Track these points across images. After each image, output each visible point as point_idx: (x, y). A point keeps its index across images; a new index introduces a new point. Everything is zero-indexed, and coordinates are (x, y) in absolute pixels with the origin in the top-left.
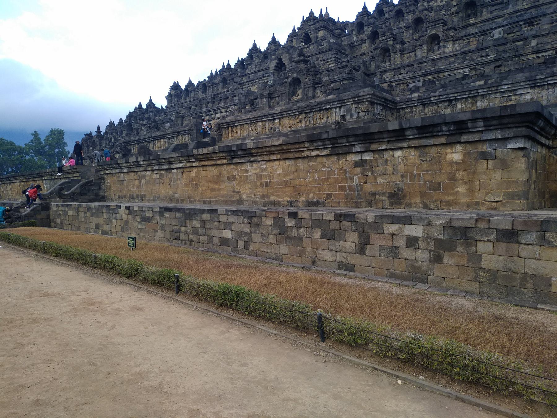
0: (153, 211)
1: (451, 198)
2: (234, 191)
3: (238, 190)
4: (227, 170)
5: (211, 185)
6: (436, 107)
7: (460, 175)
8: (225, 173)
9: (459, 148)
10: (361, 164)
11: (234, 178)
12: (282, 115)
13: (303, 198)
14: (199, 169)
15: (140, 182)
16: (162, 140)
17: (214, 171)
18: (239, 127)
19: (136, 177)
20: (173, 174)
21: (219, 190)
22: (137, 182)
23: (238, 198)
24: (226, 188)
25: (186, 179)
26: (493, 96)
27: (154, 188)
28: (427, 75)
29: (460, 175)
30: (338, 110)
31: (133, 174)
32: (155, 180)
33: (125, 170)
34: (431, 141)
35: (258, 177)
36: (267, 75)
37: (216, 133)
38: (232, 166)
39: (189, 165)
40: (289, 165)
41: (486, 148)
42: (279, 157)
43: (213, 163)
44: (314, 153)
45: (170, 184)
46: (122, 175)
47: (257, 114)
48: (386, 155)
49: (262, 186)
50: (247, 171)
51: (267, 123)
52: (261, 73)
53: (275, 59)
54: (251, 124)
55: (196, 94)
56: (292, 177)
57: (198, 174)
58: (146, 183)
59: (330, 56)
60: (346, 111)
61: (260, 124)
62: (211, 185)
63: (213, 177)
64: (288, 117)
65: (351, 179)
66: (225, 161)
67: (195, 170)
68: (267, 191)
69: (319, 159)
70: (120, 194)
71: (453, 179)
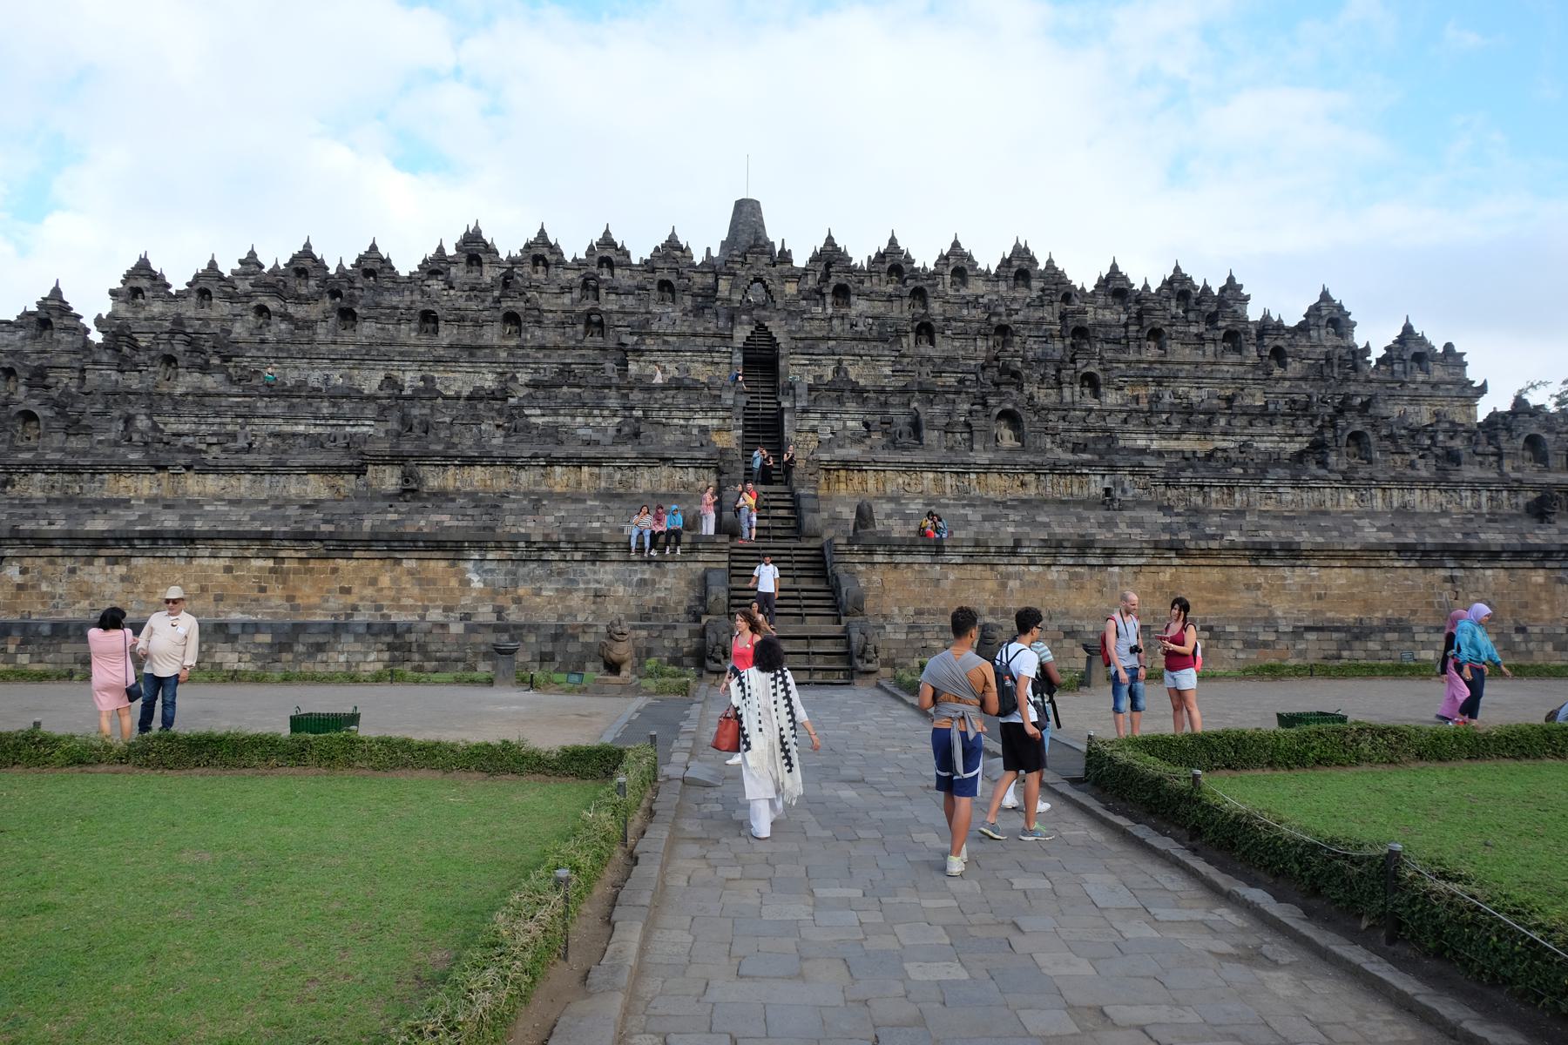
0: (1277, 631)
1: (1535, 615)
2: (1258, 605)
3: (1267, 603)
4: (1244, 575)
5: (1209, 596)
6: (1182, 491)
7: (1543, 595)
8: (1240, 578)
9: (1541, 572)
10: (1452, 579)
11: (1258, 587)
12: (987, 469)
13: (1379, 615)
14: (1180, 569)
15: (1004, 586)
16: (585, 469)
17: (1216, 575)
18: (870, 473)
19: (988, 573)
20: (1111, 574)
21: (1228, 602)
22: (991, 585)
23: (1266, 614)
24: (1241, 601)
25: (1147, 584)
26: (1252, 490)
27: (1049, 596)
28: (1089, 431)
29: (1543, 595)
30: (1098, 478)
31: (979, 568)
32: (1053, 584)
33: (959, 560)
34: (1521, 564)
35: (1304, 587)
36: (724, 349)
37: (812, 478)
38: (1254, 570)
39: (1159, 562)
40: (1356, 575)
41: (1561, 574)
42: (1345, 563)
43: (1219, 562)
44: (1397, 564)
45: (1100, 591)
46: (938, 567)
47: (918, 457)
48: (1478, 573)
49: (1311, 598)
50: (1284, 578)
51: (948, 476)
52: (709, 342)
53: (751, 324)
54: (904, 472)
55: (383, 329)
56: (1361, 589)
57: (1174, 578)
58: (1022, 586)
59: (887, 353)
60: (1114, 483)
61: (931, 475)
62: (1209, 596)
63: (1213, 583)
64: (999, 474)
65: (1440, 594)
66: (1246, 562)
67: (1169, 571)
68: (1319, 605)
69: (1400, 571)
70: (927, 606)
71: (1538, 598)
